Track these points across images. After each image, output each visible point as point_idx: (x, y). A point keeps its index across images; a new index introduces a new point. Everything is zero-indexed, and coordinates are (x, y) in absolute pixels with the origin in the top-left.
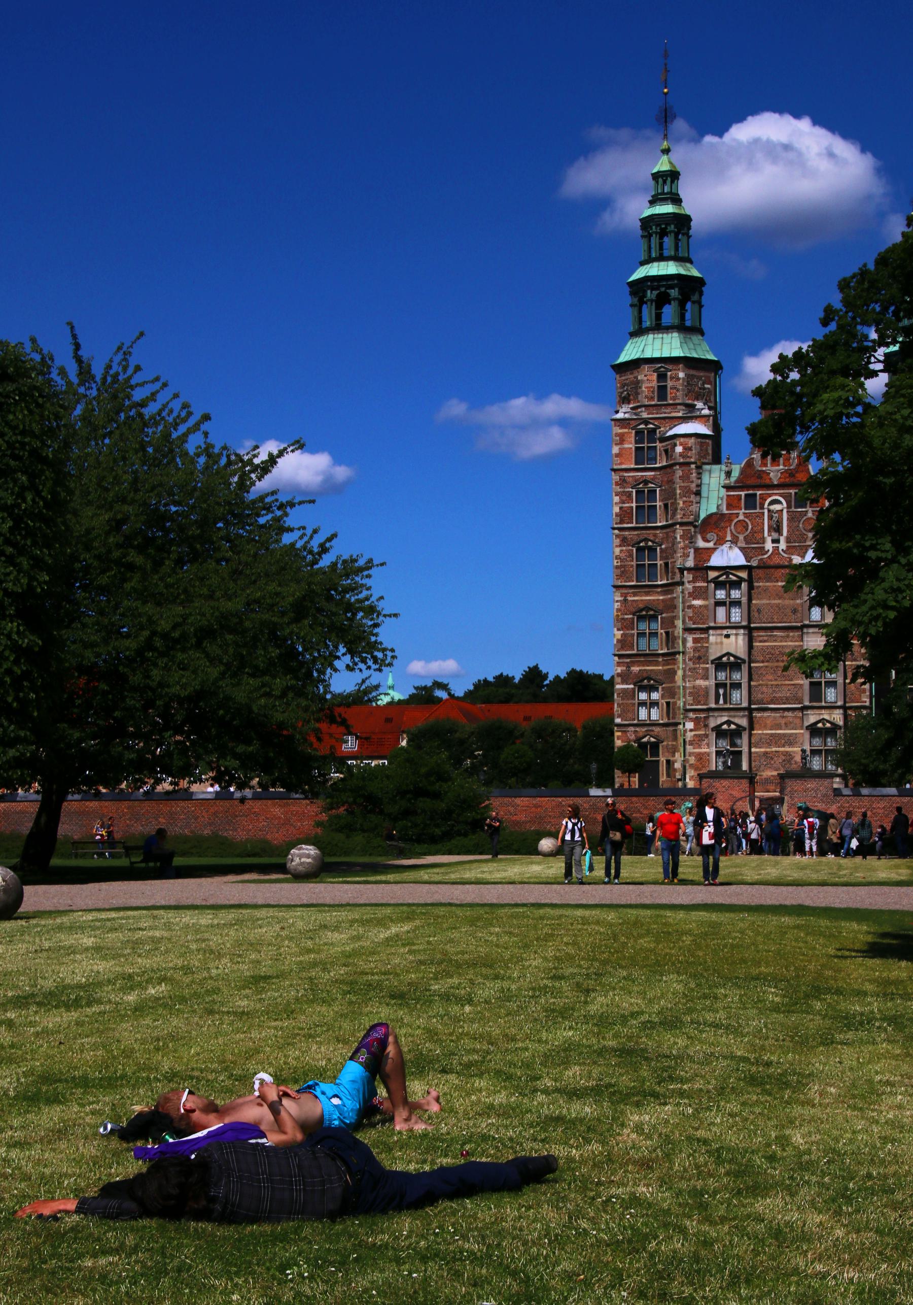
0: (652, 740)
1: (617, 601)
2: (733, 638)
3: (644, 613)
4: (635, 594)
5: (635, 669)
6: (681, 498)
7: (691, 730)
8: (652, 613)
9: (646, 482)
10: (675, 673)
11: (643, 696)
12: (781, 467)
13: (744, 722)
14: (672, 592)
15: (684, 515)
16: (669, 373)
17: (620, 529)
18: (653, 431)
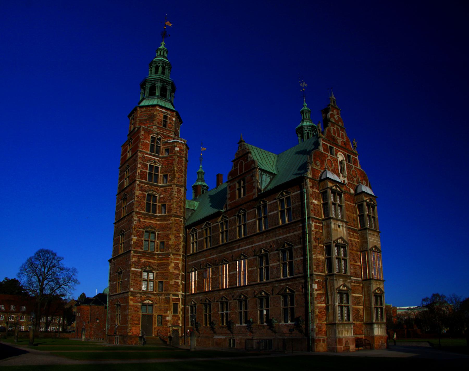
0: (150, 302)
1: (135, 220)
2: (341, 227)
3: (149, 229)
4: (145, 218)
5: (143, 260)
6: (177, 172)
7: (317, 290)
8: (153, 230)
9: (155, 162)
10: (169, 265)
11: (145, 275)
12: (341, 139)
13: (349, 285)
14: (169, 220)
15: (178, 181)
16: (169, 116)
17: (141, 182)
18: (160, 139)
